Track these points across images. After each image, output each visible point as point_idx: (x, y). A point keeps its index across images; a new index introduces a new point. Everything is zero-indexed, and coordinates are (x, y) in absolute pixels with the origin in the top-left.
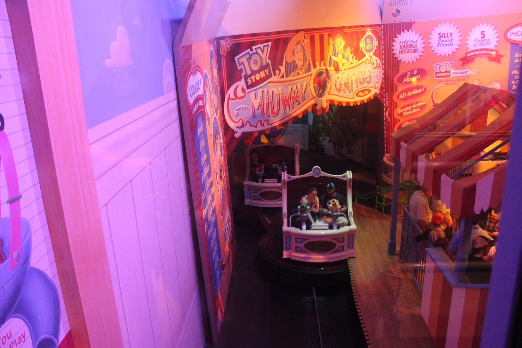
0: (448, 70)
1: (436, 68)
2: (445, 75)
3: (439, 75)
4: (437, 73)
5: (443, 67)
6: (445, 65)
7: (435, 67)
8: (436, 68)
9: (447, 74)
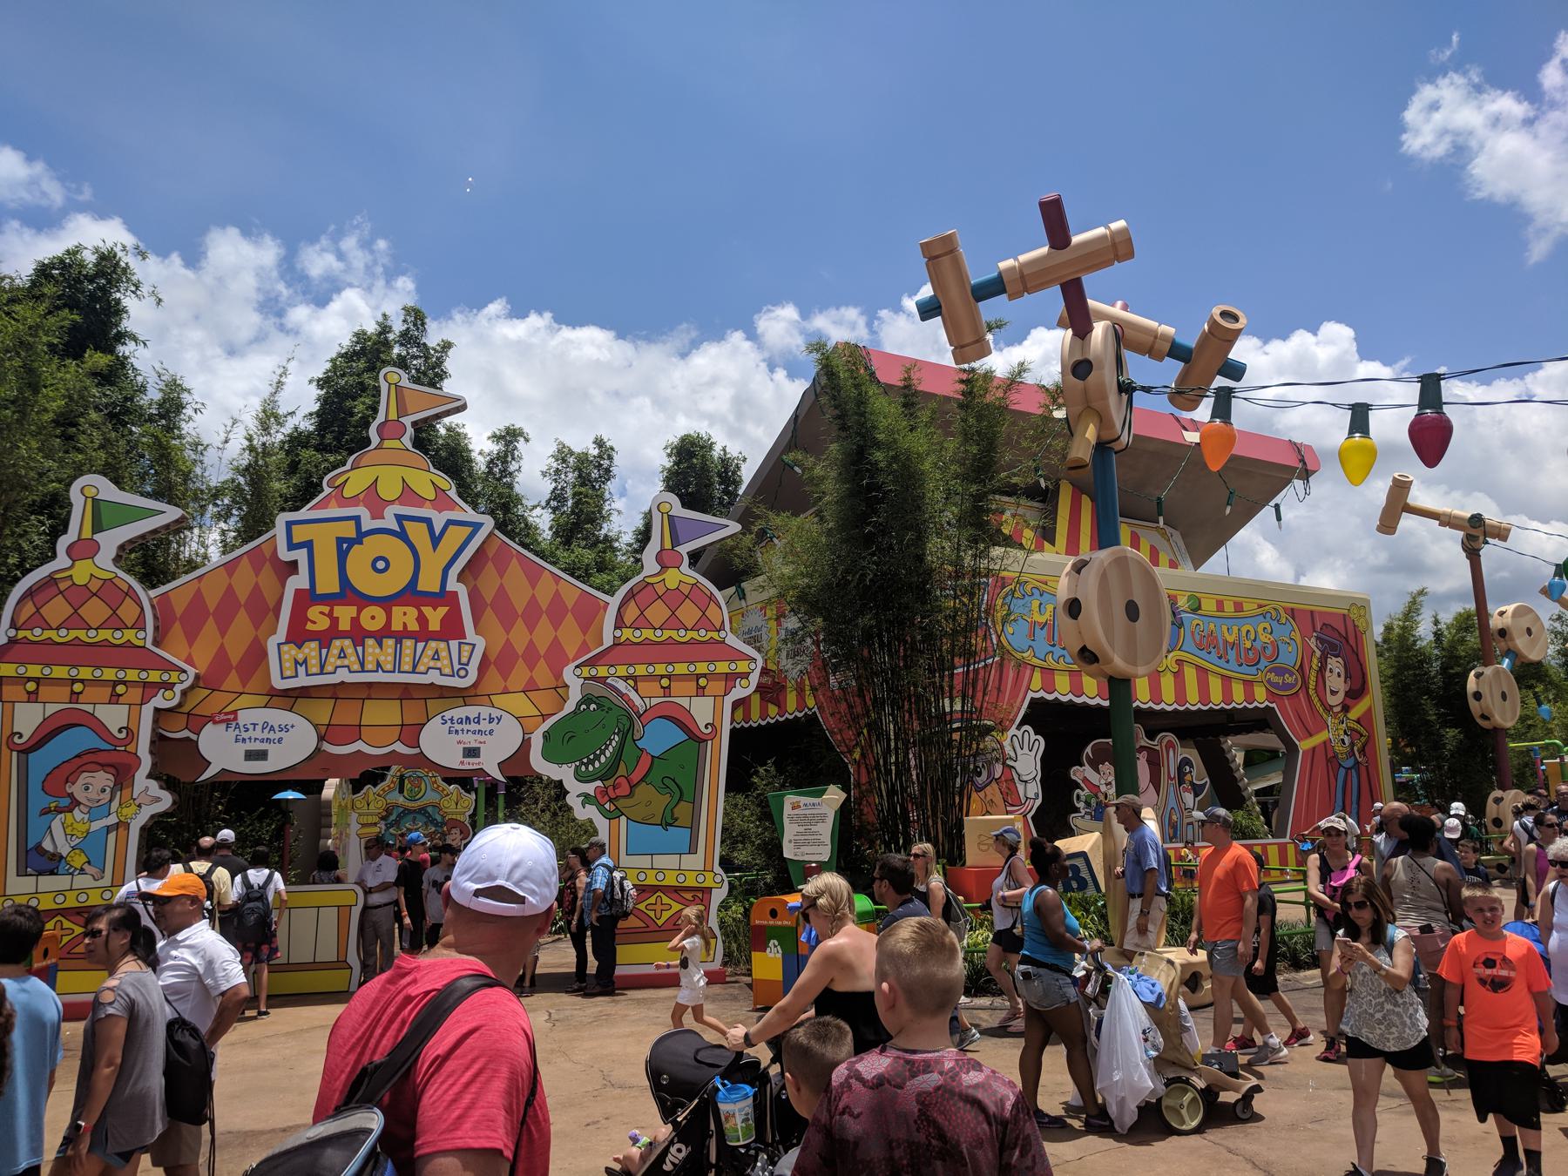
0: (428, 583)
1: (301, 555)
2: (397, 626)
3: (335, 621)
5: (373, 547)
6: (402, 535)
7: (292, 546)
8: (301, 555)
9: (422, 620)
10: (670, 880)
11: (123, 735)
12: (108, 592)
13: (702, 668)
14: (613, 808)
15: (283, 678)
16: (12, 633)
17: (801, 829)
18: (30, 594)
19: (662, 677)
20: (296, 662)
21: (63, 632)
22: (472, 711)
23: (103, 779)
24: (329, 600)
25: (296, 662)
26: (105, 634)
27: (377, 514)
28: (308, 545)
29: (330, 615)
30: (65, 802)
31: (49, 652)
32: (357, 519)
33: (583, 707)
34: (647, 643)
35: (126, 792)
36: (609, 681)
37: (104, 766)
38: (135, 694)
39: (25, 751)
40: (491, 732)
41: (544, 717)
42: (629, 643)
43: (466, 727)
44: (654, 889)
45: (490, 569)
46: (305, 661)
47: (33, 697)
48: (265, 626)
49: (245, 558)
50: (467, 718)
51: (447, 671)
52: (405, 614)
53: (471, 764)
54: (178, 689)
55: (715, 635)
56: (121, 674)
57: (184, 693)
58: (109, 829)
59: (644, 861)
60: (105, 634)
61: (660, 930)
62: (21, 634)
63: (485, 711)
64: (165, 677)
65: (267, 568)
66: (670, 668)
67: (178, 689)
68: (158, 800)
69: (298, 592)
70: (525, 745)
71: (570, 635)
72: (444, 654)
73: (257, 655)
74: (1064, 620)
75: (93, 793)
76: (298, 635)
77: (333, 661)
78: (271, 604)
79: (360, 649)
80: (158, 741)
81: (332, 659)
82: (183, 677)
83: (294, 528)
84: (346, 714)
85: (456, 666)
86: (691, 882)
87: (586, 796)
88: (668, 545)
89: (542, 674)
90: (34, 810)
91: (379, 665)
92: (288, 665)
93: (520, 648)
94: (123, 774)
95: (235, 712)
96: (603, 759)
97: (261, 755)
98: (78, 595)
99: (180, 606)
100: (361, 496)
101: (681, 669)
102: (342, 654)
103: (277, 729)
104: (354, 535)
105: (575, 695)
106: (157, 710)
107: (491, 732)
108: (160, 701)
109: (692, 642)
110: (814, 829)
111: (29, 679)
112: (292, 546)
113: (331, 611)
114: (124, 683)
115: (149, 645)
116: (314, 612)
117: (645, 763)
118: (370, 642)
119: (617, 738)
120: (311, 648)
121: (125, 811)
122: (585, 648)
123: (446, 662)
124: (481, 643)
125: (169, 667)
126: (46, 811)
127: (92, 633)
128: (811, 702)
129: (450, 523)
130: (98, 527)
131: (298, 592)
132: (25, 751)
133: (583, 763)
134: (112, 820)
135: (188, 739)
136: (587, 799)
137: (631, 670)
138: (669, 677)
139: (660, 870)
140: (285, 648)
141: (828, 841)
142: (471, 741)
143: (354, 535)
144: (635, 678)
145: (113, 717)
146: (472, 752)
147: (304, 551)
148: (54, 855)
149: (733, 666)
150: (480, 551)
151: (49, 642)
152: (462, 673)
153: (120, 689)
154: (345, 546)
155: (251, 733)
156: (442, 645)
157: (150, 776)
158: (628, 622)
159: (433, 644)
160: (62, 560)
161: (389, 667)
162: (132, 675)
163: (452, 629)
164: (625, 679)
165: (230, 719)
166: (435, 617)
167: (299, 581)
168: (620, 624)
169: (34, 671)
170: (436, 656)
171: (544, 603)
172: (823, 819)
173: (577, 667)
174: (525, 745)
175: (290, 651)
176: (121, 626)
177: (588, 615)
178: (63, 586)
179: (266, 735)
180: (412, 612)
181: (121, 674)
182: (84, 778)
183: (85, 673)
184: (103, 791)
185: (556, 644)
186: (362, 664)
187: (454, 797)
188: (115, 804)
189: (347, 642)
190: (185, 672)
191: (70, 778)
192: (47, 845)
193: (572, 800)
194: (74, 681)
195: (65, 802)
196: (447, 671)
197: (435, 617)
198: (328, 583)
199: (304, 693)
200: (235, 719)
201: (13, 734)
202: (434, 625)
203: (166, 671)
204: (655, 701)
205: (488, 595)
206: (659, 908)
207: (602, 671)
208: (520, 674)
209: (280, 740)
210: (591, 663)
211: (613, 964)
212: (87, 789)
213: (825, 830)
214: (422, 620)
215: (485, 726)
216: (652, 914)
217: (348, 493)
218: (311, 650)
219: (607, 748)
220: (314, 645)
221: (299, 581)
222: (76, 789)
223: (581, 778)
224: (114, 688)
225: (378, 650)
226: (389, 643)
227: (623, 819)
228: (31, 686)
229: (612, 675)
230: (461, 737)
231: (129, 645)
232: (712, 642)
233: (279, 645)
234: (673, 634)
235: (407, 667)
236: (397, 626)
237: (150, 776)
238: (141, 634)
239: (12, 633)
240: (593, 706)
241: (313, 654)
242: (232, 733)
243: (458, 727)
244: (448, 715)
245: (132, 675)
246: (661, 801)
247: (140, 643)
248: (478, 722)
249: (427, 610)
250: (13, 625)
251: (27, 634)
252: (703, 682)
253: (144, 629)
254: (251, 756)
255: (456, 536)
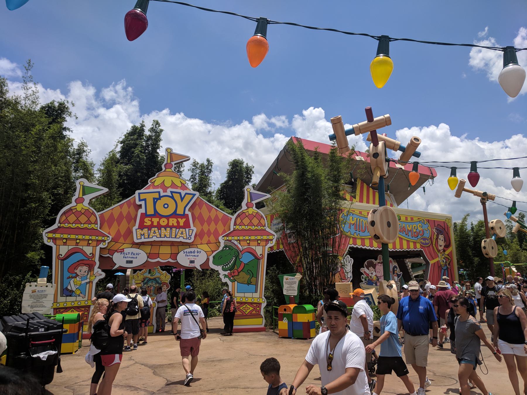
0: (180, 211)
1: (143, 203)
2: (170, 224)
3: (152, 222)
4: (144, 216)
5: (164, 200)
6: (172, 197)
7: (140, 200)
8: (143, 203)
9: (178, 222)
10: (250, 301)
11: (91, 255)
12: (87, 213)
13: (259, 238)
14: (233, 279)
15: (137, 239)
16: (59, 225)
17: (289, 286)
18: (64, 213)
19: (247, 240)
20: (141, 234)
21: (74, 225)
22: (192, 250)
23: (85, 268)
24: (151, 216)
25: (141, 234)
26: (86, 226)
27: (165, 191)
28: (145, 200)
29: (151, 221)
30: (74, 275)
31: (70, 231)
32: (159, 192)
33: (225, 249)
34: (243, 230)
35: (92, 272)
36: (232, 241)
37: (85, 265)
38: (95, 243)
39: (63, 260)
40: (198, 256)
41: (213, 252)
42: (238, 230)
43: (190, 254)
44: (245, 303)
45: (197, 207)
46: (144, 234)
47: (65, 244)
48: (131, 224)
49: (125, 203)
50: (191, 252)
51: (185, 237)
52: (173, 220)
53: (192, 265)
54: (107, 242)
55: (263, 228)
56: (90, 237)
57: (108, 243)
58: (87, 283)
59: (242, 295)
60: (86, 226)
61: (247, 315)
62: (62, 225)
63: (196, 250)
64: (103, 238)
65: (132, 206)
66: (250, 238)
67: (107, 242)
68: (101, 275)
69: (142, 214)
70: (208, 259)
71: (220, 227)
72: (184, 233)
73: (129, 232)
74: (370, 227)
75: (82, 272)
76: (142, 226)
77: (152, 234)
78: (133, 216)
79: (160, 231)
80: (101, 257)
81: (151, 234)
82: (108, 238)
83: (141, 194)
84: (155, 250)
85: (188, 236)
86: (256, 301)
87: (225, 275)
88: (249, 201)
89: (212, 239)
90: (65, 277)
91: (165, 236)
92: (139, 235)
93: (206, 231)
94: (91, 267)
95: (123, 249)
96: (230, 264)
97: (131, 262)
98: (78, 214)
99: (106, 217)
100: (160, 185)
101: (253, 238)
102: (155, 232)
103: (135, 254)
104: (158, 197)
105: (222, 245)
106: (101, 248)
107: (198, 256)
108: (102, 245)
109: (256, 230)
110: (292, 286)
111: (64, 239)
112: (140, 200)
113: (151, 220)
114: (91, 240)
115: (99, 229)
116: (146, 220)
117: (242, 265)
118: (163, 229)
119: (234, 258)
120: (145, 230)
121: (92, 278)
122: (224, 231)
123: (185, 235)
124: (195, 230)
125: (104, 235)
126: (69, 278)
127: (82, 225)
128: (281, 247)
129: (186, 194)
130: (84, 194)
131: (142, 214)
132: (63, 260)
133: (224, 265)
134: (88, 280)
135: (109, 257)
136: (225, 276)
137: (238, 238)
138: (249, 240)
139: (247, 298)
140: (138, 230)
141: (297, 290)
142: (192, 258)
143: (158, 197)
144: (240, 240)
145: (88, 250)
146: (192, 262)
147: (144, 202)
148: (71, 291)
149: (268, 237)
150: (195, 202)
151: (70, 228)
152: (190, 238)
153: (90, 242)
154: (156, 200)
155: (128, 256)
156: (184, 230)
157: (99, 268)
158: (238, 223)
159: (181, 230)
160: (73, 204)
161: (168, 236)
162: (94, 238)
163: (187, 225)
164: (237, 240)
165: (122, 251)
166: (182, 221)
167: (142, 211)
168: (235, 224)
169: (65, 236)
170: (182, 233)
171: (213, 218)
172: (295, 283)
173: (223, 237)
174: (208, 259)
175: (139, 231)
176: (91, 223)
177: (226, 221)
178: (74, 211)
179: (132, 256)
180: (175, 220)
181: (90, 237)
182: (80, 268)
183: (80, 237)
184: (85, 272)
185: (216, 230)
186: (160, 235)
187: (165, 275)
188: (89, 276)
189: (156, 229)
190: (109, 237)
191: (76, 268)
192: (69, 288)
193: (221, 276)
194: (77, 239)
195: (74, 275)
196: (185, 237)
197: (182, 221)
198: (151, 211)
199: (143, 244)
200: (123, 251)
201: (59, 255)
202: (182, 224)
203: (103, 237)
204: (245, 247)
205: (197, 215)
206: (246, 309)
207: (230, 238)
208: (206, 238)
209: (136, 258)
210: (227, 236)
211: (232, 325)
212: (81, 271)
213: (296, 286)
214: (178, 222)
215: (196, 254)
216: (244, 310)
217: (156, 184)
218: (146, 231)
219: (231, 261)
220: (146, 229)
221: (142, 211)
222: (77, 271)
223: (224, 270)
224: (88, 241)
225: (165, 231)
226: (168, 229)
227: (236, 282)
228: (64, 241)
229: (233, 239)
230: (189, 257)
231: (93, 229)
232: (262, 230)
233: (136, 229)
234: (251, 227)
235: (173, 236)
236: (170, 224)
237: (99, 268)
238: (96, 226)
239: (59, 225)
240: (227, 249)
241: (146, 232)
242: (122, 255)
243: (188, 254)
244: (185, 251)
245: (94, 238)
246: (247, 277)
247: (96, 228)
248: (194, 253)
249: (179, 220)
250: (59, 222)
251: (64, 225)
252: (259, 242)
253: (97, 224)
254: (128, 262)
255: (188, 197)
